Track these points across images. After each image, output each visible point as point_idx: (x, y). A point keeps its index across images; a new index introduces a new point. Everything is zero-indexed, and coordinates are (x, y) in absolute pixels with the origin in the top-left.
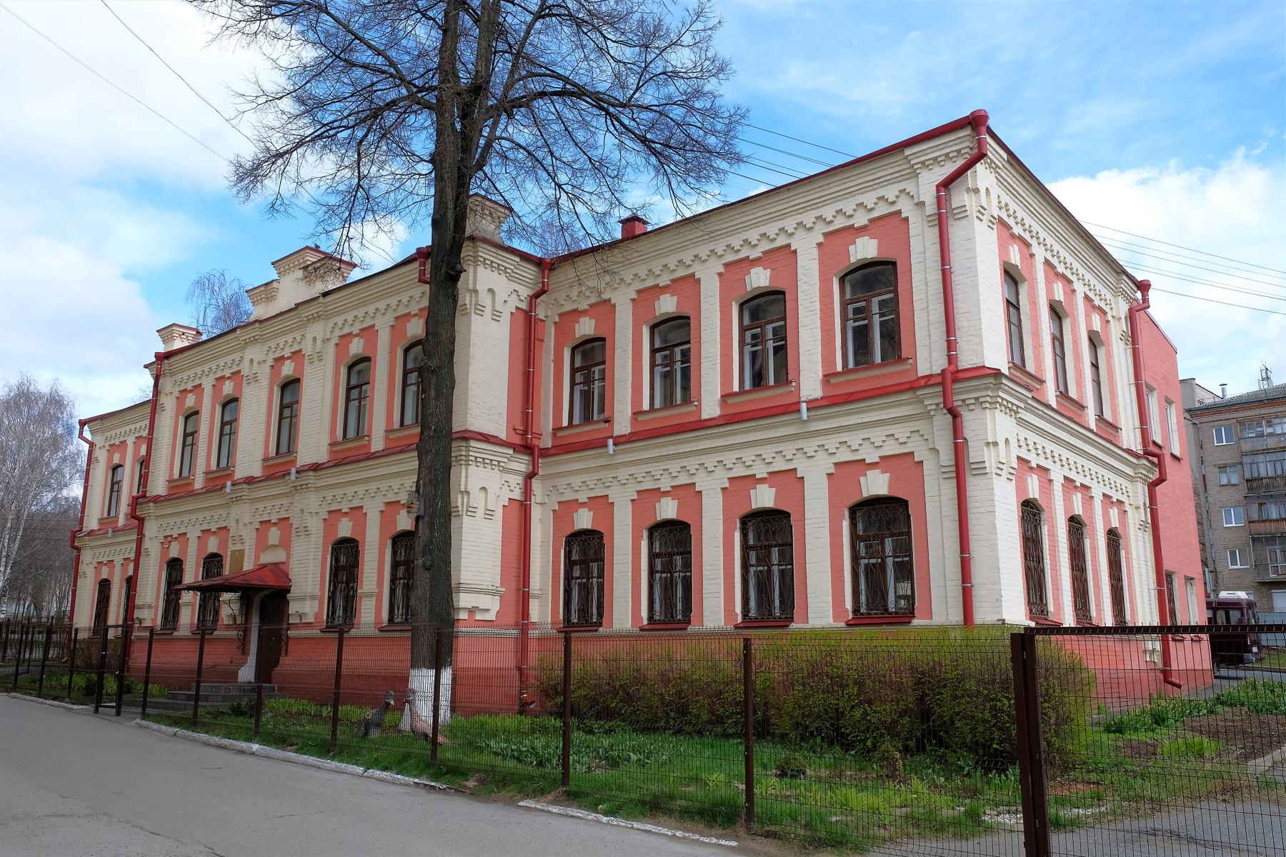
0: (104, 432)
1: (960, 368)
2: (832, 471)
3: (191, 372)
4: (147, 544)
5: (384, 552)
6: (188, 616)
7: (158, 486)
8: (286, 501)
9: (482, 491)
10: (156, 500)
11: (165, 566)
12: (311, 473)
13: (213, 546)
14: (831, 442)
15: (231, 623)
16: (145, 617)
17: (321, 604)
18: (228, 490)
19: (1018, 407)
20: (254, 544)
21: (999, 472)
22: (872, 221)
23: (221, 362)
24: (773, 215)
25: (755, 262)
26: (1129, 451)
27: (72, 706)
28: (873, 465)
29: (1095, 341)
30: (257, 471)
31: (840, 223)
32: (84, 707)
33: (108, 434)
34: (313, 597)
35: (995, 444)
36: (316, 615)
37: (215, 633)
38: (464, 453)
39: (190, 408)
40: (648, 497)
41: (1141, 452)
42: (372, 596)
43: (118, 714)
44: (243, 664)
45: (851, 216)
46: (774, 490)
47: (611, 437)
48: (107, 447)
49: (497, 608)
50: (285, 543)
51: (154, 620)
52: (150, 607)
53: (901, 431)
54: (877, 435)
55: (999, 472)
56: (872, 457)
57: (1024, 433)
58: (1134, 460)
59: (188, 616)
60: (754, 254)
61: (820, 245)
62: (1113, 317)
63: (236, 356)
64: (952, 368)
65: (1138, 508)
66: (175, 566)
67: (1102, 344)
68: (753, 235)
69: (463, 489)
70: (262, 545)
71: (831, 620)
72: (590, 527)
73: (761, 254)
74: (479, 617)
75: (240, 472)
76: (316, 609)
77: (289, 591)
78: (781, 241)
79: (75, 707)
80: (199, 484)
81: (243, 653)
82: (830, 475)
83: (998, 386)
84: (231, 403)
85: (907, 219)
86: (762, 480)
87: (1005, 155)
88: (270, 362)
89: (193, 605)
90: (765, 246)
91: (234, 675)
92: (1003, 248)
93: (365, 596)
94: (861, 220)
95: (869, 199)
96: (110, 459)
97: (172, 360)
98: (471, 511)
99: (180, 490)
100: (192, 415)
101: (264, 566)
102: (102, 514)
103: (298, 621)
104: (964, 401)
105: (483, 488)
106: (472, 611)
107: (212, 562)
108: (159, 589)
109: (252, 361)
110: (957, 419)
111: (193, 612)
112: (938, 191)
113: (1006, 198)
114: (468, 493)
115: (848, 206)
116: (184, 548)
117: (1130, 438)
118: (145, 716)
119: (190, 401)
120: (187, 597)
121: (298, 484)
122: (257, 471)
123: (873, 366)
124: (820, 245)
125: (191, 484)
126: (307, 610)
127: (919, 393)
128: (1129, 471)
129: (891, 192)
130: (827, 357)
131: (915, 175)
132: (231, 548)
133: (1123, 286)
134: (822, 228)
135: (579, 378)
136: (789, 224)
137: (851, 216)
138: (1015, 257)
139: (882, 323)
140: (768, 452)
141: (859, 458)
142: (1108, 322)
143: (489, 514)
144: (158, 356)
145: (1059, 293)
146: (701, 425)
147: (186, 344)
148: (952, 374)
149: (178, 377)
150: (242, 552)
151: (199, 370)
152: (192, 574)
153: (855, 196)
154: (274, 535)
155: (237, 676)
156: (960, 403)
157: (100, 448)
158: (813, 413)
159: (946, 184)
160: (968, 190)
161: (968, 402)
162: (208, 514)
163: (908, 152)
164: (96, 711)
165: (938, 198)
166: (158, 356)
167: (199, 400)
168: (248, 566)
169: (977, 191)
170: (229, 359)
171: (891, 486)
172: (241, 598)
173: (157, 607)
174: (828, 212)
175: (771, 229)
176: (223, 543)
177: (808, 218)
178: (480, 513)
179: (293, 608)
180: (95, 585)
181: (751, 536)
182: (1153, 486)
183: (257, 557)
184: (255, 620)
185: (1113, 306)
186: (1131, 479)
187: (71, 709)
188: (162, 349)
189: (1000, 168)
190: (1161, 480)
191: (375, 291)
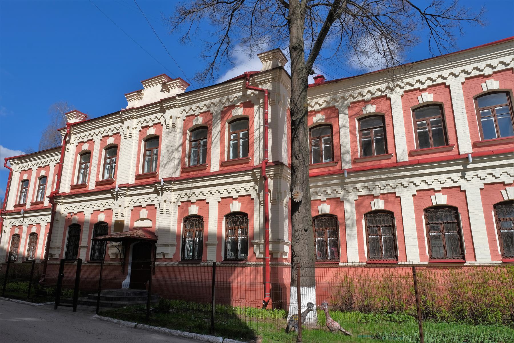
0: (19, 164)
2: (483, 187)
5: (222, 223)
7: (65, 188)
11: (68, 228)
14: (482, 173)
15: (114, 257)
16: (56, 253)
17: (178, 249)
20: (130, 217)
24: (436, 69)
25: (424, 90)
27: (35, 304)
30: (131, 181)
31: (475, 73)
32: (40, 304)
34: (173, 245)
36: (174, 255)
38: (280, 173)
42: (215, 245)
43: (75, 310)
44: (124, 279)
46: (446, 196)
48: (20, 171)
51: (61, 255)
52: (58, 248)
60: (422, 87)
61: (463, 83)
71: (490, 260)
76: (175, 252)
77: (156, 242)
78: (440, 81)
79: (37, 304)
80: (92, 186)
81: (123, 273)
82: (481, 189)
89: (88, 248)
90: (430, 83)
91: (119, 285)
93: (209, 245)
102: (16, 203)
103: (162, 257)
108: (64, 240)
111: (88, 251)
115: (481, 65)
118: (97, 313)
119: (85, 147)
122: (131, 181)
124: (463, 83)
126: (169, 252)
130: (473, 135)
134: (464, 76)
141: (501, 181)
146: (398, 166)
153: (472, 64)
155: (121, 285)
157: (16, 172)
164: (56, 308)
172: (123, 245)
179: (159, 250)
180: (10, 237)
184: (130, 258)
187: (34, 306)
191: (191, 99)
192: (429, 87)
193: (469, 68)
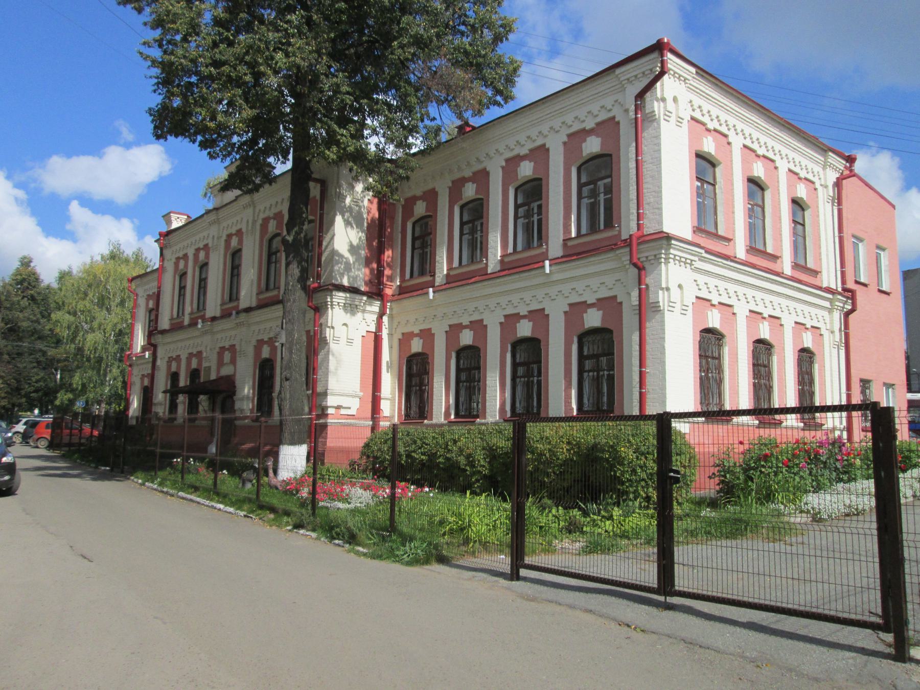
1: (645, 233)
3: (180, 245)
4: (159, 362)
6: (182, 410)
8: (233, 333)
9: (344, 327)
10: (163, 332)
12: (244, 314)
13: (194, 365)
18: (199, 326)
19: (692, 261)
21: (670, 309)
22: (598, 124)
23: (197, 237)
26: (828, 290)
28: (592, 305)
29: (797, 204)
30: (218, 314)
33: (146, 287)
35: (668, 289)
37: (197, 422)
39: (182, 270)
40: (454, 330)
41: (840, 289)
44: (211, 442)
45: (584, 121)
47: (433, 286)
48: (145, 297)
49: (358, 406)
50: (233, 361)
53: (609, 280)
54: (594, 282)
55: (670, 309)
56: (591, 301)
57: (702, 279)
58: (830, 296)
59: (182, 410)
62: (821, 185)
63: (205, 234)
64: (640, 233)
65: (832, 332)
66: (175, 377)
67: (809, 207)
68: (522, 138)
69: (329, 325)
70: (221, 364)
72: (420, 350)
73: (528, 152)
74: (343, 412)
75: (209, 314)
80: (186, 322)
83: (669, 246)
84: (204, 266)
85: (618, 123)
86: (524, 317)
87: (693, 70)
88: (224, 237)
90: (531, 145)
92: (694, 138)
94: (590, 124)
95: (595, 107)
96: (147, 304)
97: (170, 237)
98: (337, 340)
99: (177, 327)
100: (183, 275)
101: (221, 378)
104: (647, 257)
105: (345, 324)
106: (338, 407)
107: (194, 374)
109: (213, 237)
110: (643, 272)
112: (636, 100)
113: (697, 101)
114: (333, 328)
115: (582, 113)
116: (179, 367)
117: (830, 277)
120: (181, 398)
121: (238, 321)
123: (600, 231)
124: (565, 143)
125: (183, 322)
127: (618, 252)
128: (827, 304)
129: (608, 102)
131: (623, 89)
132: (205, 364)
133: (829, 160)
135: (418, 243)
136: (545, 129)
137: (584, 121)
138: (709, 146)
139: (605, 200)
140: (527, 296)
142: (816, 189)
143: (350, 342)
144: (161, 234)
145: (759, 170)
147: (180, 224)
148: (639, 238)
149: (174, 248)
150: (209, 368)
151: (185, 243)
152: (182, 382)
154: (227, 356)
156: (644, 259)
158: (553, 268)
159: (641, 96)
160: (657, 100)
161: (649, 258)
162: (191, 342)
163: (618, 71)
165: (636, 106)
166: (161, 234)
167: (186, 266)
168: (213, 376)
169: (663, 100)
170: (201, 235)
171: (603, 320)
173: (165, 404)
174: (569, 119)
175: (533, 133)
176: (200, 363)
177: (557, 124)
178: (343, 340)
181: (518, 356)
182: (847, 314)
183: (218, 371)
185: (822, 176)
186: (830, 311)
188: (165, 229)
189: (689, 80)
190: (852, 311)
192: (531, 151)
193: (569, 119)
